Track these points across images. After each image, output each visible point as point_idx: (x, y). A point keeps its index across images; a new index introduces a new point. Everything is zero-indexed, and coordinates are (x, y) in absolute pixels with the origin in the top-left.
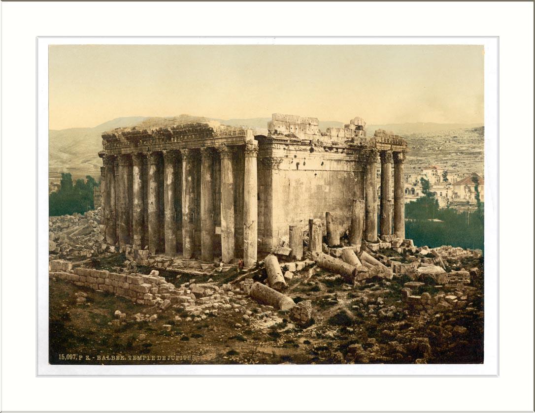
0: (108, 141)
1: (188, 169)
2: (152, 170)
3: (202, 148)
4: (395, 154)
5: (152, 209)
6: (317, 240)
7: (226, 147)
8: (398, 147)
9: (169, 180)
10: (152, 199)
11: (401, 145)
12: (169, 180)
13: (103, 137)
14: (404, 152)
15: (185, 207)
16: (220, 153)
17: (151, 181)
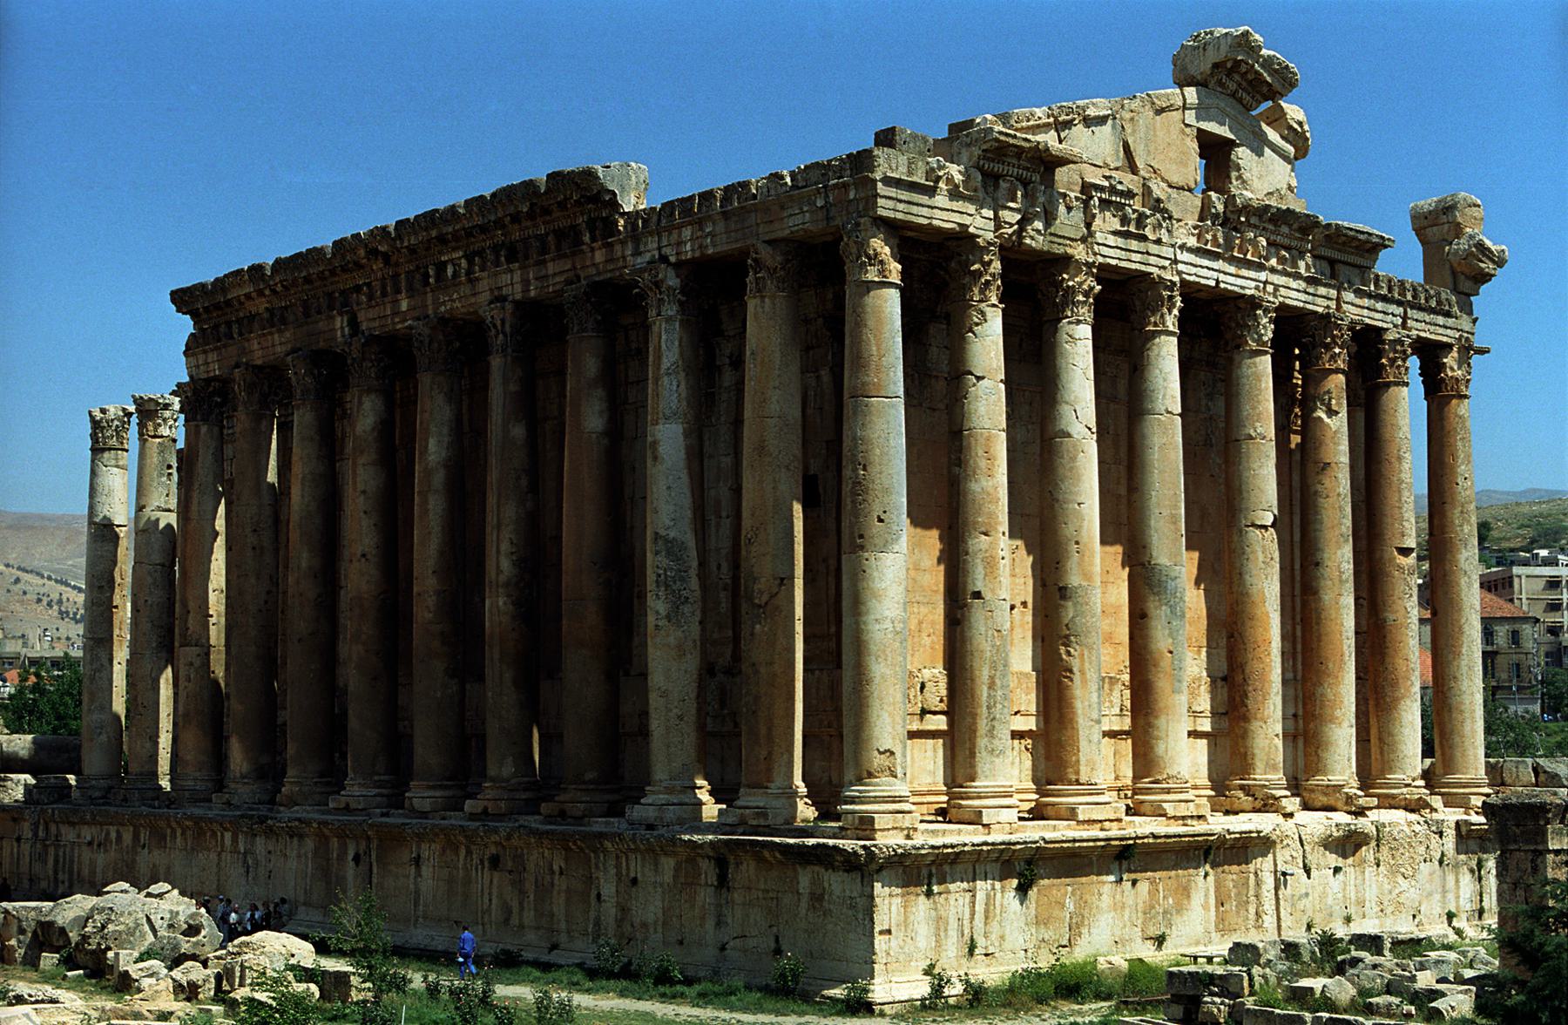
0: (194, 315)
1: (513, 388)
2: (365, 415)
4: (1430, 353)
6: (1077, 677)
7: (671, 273)
8: (1440, 320)
9: (434, 449)
10: (360, 533)
11: (1448, 315)
12: (434, 449)
13: (183, 299)
14: (1468, 350)
15: (498, 552)
16: (643, 296)
17: (361, 460)
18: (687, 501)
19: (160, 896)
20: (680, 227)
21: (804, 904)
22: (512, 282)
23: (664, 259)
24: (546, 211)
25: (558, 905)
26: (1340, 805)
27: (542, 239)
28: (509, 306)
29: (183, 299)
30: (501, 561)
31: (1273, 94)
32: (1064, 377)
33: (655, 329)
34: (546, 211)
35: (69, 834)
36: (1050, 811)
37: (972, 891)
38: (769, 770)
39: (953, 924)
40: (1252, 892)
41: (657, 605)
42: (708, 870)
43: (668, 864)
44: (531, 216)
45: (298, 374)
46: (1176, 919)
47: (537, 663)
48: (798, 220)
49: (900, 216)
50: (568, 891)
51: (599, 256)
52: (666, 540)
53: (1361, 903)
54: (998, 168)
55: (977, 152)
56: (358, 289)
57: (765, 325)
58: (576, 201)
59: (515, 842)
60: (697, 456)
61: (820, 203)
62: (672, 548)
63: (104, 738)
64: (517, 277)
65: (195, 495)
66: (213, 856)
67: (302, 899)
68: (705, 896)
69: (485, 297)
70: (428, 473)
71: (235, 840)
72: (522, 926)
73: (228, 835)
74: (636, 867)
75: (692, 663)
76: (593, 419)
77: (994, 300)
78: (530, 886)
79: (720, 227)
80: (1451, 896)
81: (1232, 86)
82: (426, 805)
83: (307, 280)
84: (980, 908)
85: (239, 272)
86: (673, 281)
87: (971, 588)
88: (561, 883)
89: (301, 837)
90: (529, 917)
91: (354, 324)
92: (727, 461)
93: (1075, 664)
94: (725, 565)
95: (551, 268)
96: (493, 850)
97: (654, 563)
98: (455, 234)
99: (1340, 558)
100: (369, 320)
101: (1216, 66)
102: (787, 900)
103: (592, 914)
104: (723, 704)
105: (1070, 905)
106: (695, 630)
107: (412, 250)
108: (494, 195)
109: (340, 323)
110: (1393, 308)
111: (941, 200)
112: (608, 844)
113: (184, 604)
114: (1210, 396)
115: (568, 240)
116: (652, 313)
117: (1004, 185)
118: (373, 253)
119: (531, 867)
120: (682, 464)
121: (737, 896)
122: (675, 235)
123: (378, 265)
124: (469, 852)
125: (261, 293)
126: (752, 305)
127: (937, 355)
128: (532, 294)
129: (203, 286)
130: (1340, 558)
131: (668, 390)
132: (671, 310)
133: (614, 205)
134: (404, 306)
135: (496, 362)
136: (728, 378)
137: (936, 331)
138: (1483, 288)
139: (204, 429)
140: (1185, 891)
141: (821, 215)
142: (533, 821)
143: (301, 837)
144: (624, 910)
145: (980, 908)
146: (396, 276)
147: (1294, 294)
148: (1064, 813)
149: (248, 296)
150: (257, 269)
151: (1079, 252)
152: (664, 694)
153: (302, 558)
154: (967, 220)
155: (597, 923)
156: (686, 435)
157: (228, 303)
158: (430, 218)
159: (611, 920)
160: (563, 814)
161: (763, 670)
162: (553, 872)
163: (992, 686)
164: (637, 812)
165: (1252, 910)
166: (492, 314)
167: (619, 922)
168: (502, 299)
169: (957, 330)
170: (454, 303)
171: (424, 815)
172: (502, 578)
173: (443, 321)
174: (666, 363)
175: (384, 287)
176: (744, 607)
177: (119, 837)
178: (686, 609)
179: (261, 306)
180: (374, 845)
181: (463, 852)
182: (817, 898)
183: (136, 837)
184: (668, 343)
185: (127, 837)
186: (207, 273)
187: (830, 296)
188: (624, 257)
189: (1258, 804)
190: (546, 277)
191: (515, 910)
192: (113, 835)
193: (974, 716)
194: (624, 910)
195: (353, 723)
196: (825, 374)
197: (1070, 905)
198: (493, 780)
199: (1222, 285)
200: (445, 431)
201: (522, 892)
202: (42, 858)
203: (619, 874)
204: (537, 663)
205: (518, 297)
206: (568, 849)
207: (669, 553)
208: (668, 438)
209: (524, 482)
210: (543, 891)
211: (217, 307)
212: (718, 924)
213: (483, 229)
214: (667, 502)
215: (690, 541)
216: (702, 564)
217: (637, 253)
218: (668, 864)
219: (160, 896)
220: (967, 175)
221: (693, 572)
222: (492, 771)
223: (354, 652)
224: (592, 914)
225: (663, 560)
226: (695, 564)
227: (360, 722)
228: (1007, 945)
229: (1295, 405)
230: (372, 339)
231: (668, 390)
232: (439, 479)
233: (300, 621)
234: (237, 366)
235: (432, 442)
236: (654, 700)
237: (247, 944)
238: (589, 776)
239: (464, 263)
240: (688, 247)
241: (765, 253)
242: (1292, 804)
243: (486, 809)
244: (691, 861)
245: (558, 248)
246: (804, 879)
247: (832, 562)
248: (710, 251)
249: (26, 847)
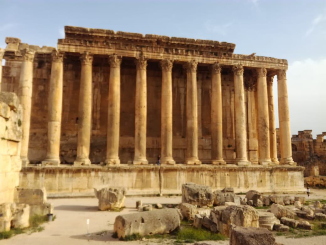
13: (67, 29)
20: (246, 60)
21: (290, 178)
22: (199, 59)
67: (130, 185)
102: (286, 177)
103: (238, 183)
121: (275, 177)
162: (225, 175)
168: (194, 61)
182: (292, 177)
188: (231, 62)
205: (200, 61)
212: (271, 182)
240: (248, 64)
246: (290, 174)
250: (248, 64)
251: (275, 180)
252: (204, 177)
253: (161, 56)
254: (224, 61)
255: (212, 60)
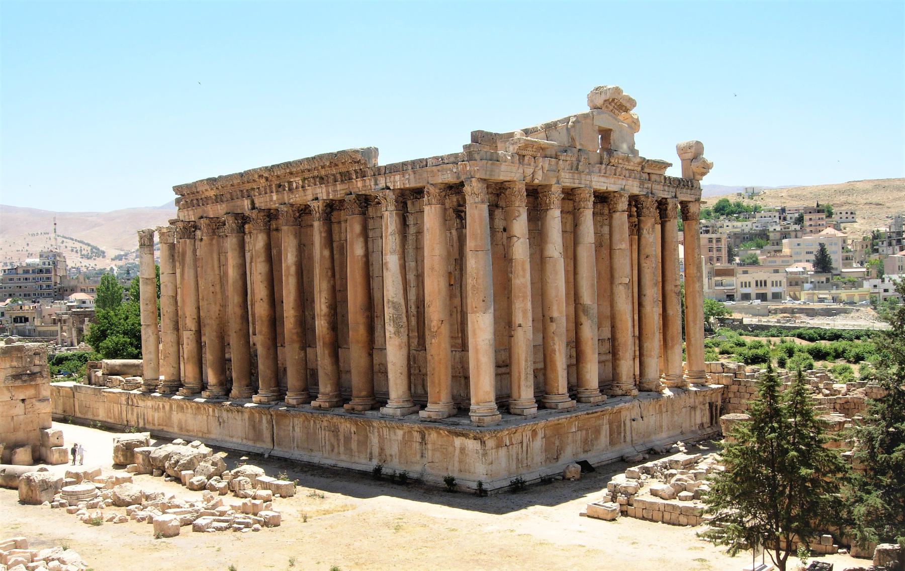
1: (323, 235)
3: (347, 198)
4: (684, 205)
5: (260, 309)
6: (557, 353)
7: (391, 193)
9: (289, 258)
12: (289, 258)
13: (177, 189)
17: (258, 260)
18: (401, 287)
19: (197, 447)
21: (457, 451)
22: (323, 193)
23: (388, 188)
24: (336, 165)
25: (354, 445)
26: (654, 388)
27: (333, 175)
28: (321, 202)
29: (177, 189)
30: (321, 305)
31: (627, 110)
32: (550, 234)
33: (385, 216)
34: (336, 165)
35: (141, 404)
36: (547, 405)
37: (522, 443)
38: (439, 396)
39: (515, 457)
40: (622, 429)
41: (390, 329)
42: (417, 436)
43: (400, 433)
44: (330, 167)
45: (230, 222)
46: (595, 443)
47: (337, 344)
48: (446, 177)
49: (487, 177)
50: (359, 441)
51: (360, 184)
52: (393, 303)
53: (661, 427)
54: (524, 153)
55: (516, 147)
56: (253, 189)
57: (431, 217)
58: (349, 165)
59: (335, 420)
60: (403, 268)
61: (455, 170)
62: (395, 306)
63: (152, 365)
64: (324, 190)
65: (186, 270)
66: (205, 417)
68: (416, 446)
69: (310, 197)
70: (288, 268)
71: (214, 411)
72: (339, 453)
73: (211, 410)
74: (385, 432)
75: (404, 351)
76: (358, 250)
77: (524, 204)
78: (341, 437)
79: (412, 176)
80: (693, 420)
81: (611, 108)
82: (294, 402)
83: (232, 185)
84: (524, 448)
85: (202, 181)
86: (391, 196)
87: (517, 323)
88: (355, 438)
89: (242, 412)
90: (342, 449)
91: (253, 203)
92: (413, 264)
93: (557, 347)
94: (413, 307)
95: (339, 187)
96: (325, 424)
97: (389, 312)
98: (297, 173)
99: (652, 293)
100: (260, 202)
101: (605, 101)
102: (450, 449)
103: (369, 451)
104: (415, 363)
105: (557, 443)
106: (406, 337)
107: (278, 176)
108: (314, 158)
109: (247, 203)
110: (671, 189)
111: (503, 167)
112: (375, 424)
113: (184, 314)
114: (601, 226)
115: (346, 177)
116: (384, 209)
117: (526, 158)
118: (261, 176)
119: (341, 430)
120: (398, 271)
121: (429, 446)
122: (392, 179)
123: (263, 181)
124: (314, 422)
125: (212, 189)
126: (427, 209)
127: (499, 224)
128: (331, 197)
129: (187, 186)
130: (652, 293)
131: (390, 241)
132: (391, 207)
133: (365, 164)
134: (275, 198)
135: (316, 224)
136: (412, 230)
137: (498, 213)
138: (704, 178)
139: (188, 241)
140: (597, 431)
141: (455, 175)
142: (341, 411)
143: (242, 412)
144: (382, 449)
145: (524, 448)
146: (270, 186)
147: (636, 190)
148: (553, 405)
149: (206, 190)
150: (212, 181)
151: (553, 181)
152: (394, 364)
153: (234, 299)
154: (513, 175)
155: (371, 453)
156: (399, 260)
157: (198, 192)
158: (288, 164)
159: (377, 454)
160: (353, 409)
161: (436, 358)
163: (526, 361)
164: (384, 410)
165: (622, 435)
166: (314, 205)
167: (380, 455)
168: (317, 199)
169: (509, 218)
170: (298, 198)
171: (294, 406)
172: (323, 313)
173: (292, 205)
174: (390, 230)
175: (265, 189)
176: (427, 333)
177: (164, 407)
178: (402, 330)
179: (211, 193)
180: (274, 417)
181: (312, 422)
182: (463, 450)
183: (171, 407)
184: (390, 221)
185: (167, 407)
186: (190, 180)
187: (455, 200)
189: (624, 392)
190: (336, 191)
191: (336, 446)
192: (161, 406)
193: (519, 373)
194: (382, 449)
195: (261, 367)
196: (454, 232)
197: (557, 443)
198: (323, 394)
199: (609, 189)
200: (294, 250)
201: (338, 440)
202: (132, 414)
203: (379, 435)
204: (337, 344)
205: (325, 198)
206: (357, 425)
207: (394, 308)
208: (392, 261)
209: (330, 274)
210: (348, 439)
211: (193, 193)
213: (309, 171)
214: (391, 288)
215: (402, 302)
216: (407, 312)
217: (376, 184)
218: (400, 433)
219: (197, 447)
220: (512, 156)
221: (404, 315)
222: (322, 389)
223: (259, 340)
224: (369, 451)
225: (391, 311)
226: (405, 311)
227: (263, 367)
228: (535, 461)
229: (636, 229)
230: (260, 210)
231: (390, 241)
232: (293, 270)
233: (234, 326)
234: (202, 217)
235: (289, 255)
236: (390, 367)
237: (238, 472)
238: (364, 393)
239: (300, 182)
241: (432, 189)
242: (635, 392)
243: (320, 406)
244: (410, 432)
245: (342, 181)
246: (458, 441)
247: (459, 309)
248: (408, 186)
249: (124, 408)
250: (398, 182)
251: (430, 453)
252: (323, 432)
253: (273, 200)
254: (358, 185)
255: (338, 191)
